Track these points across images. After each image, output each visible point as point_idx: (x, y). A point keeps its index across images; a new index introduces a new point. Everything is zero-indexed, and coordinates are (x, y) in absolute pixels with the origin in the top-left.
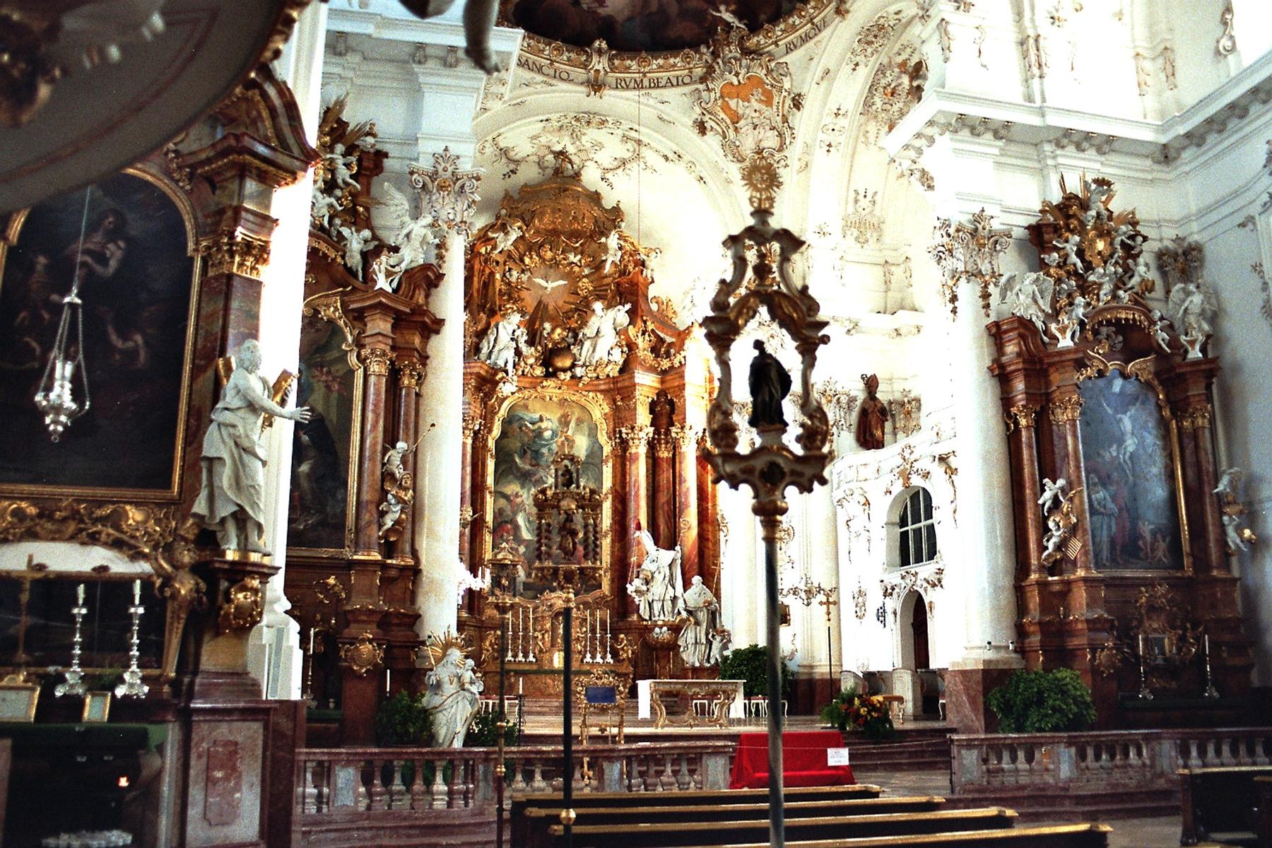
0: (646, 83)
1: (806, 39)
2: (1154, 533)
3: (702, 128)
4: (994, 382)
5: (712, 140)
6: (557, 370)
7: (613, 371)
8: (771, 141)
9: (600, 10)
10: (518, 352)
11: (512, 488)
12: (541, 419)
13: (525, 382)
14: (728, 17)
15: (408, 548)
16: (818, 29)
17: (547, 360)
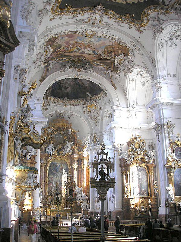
0: (74, 105)
1: (101, 99)
2: (144, 191)
3: (84, 113)
4: (120, 168)
5: (86, 115)
6: (60, 154)
7: (70, 154)
8: (96, 115)
9: (66, 92)
10: (53, 151)
11: (52, 176)
12: (57, 163)
13: (54, 156)
14: (88, 94)
15: (32, 195)
16: (103, 97)
17: (58, 152)
